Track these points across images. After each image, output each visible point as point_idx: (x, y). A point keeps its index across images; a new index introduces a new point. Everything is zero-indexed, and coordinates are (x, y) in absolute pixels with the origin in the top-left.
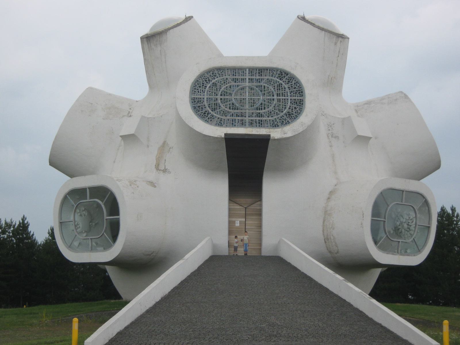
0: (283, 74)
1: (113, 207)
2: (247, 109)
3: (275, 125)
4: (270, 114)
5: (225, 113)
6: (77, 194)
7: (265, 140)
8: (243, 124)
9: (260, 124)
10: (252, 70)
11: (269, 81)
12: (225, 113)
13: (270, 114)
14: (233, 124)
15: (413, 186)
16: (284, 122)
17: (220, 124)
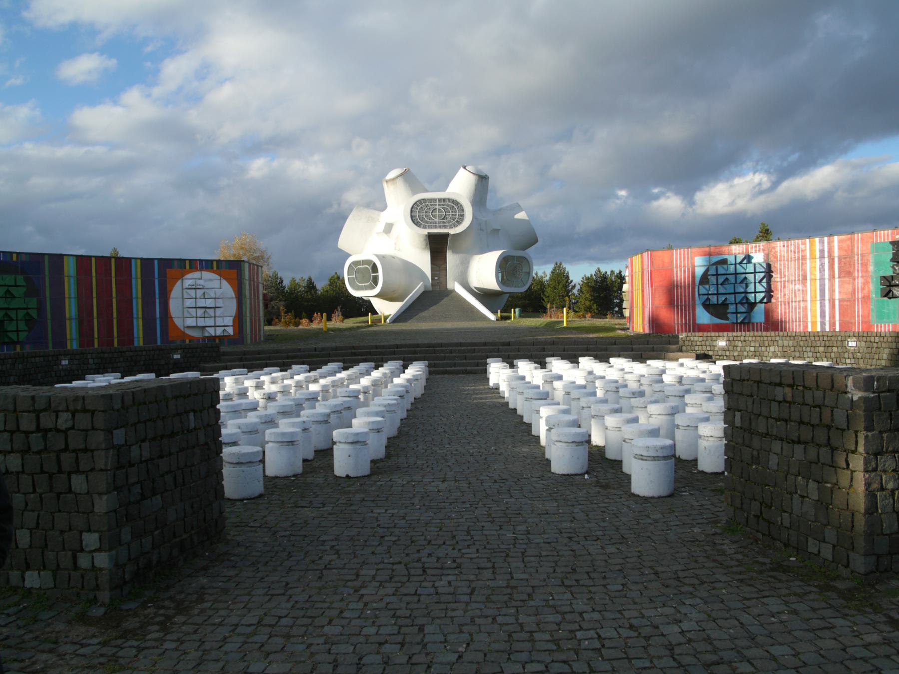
0: (454, 201)
1: (374, 268)
2: (437, 220)
3: (451, 227)
4: (449, 222)
5: (427, 222)
6: (356, 263)
7: (445, 236)
8: (435, 227)
9: (444, 227)
10: (439, 200)
11: (448, 205)
12: (427, 222)
13: (449, 222)
14: (431, 227)
15: (520, 253)
16: (455, 226)
17: (424, 227)
